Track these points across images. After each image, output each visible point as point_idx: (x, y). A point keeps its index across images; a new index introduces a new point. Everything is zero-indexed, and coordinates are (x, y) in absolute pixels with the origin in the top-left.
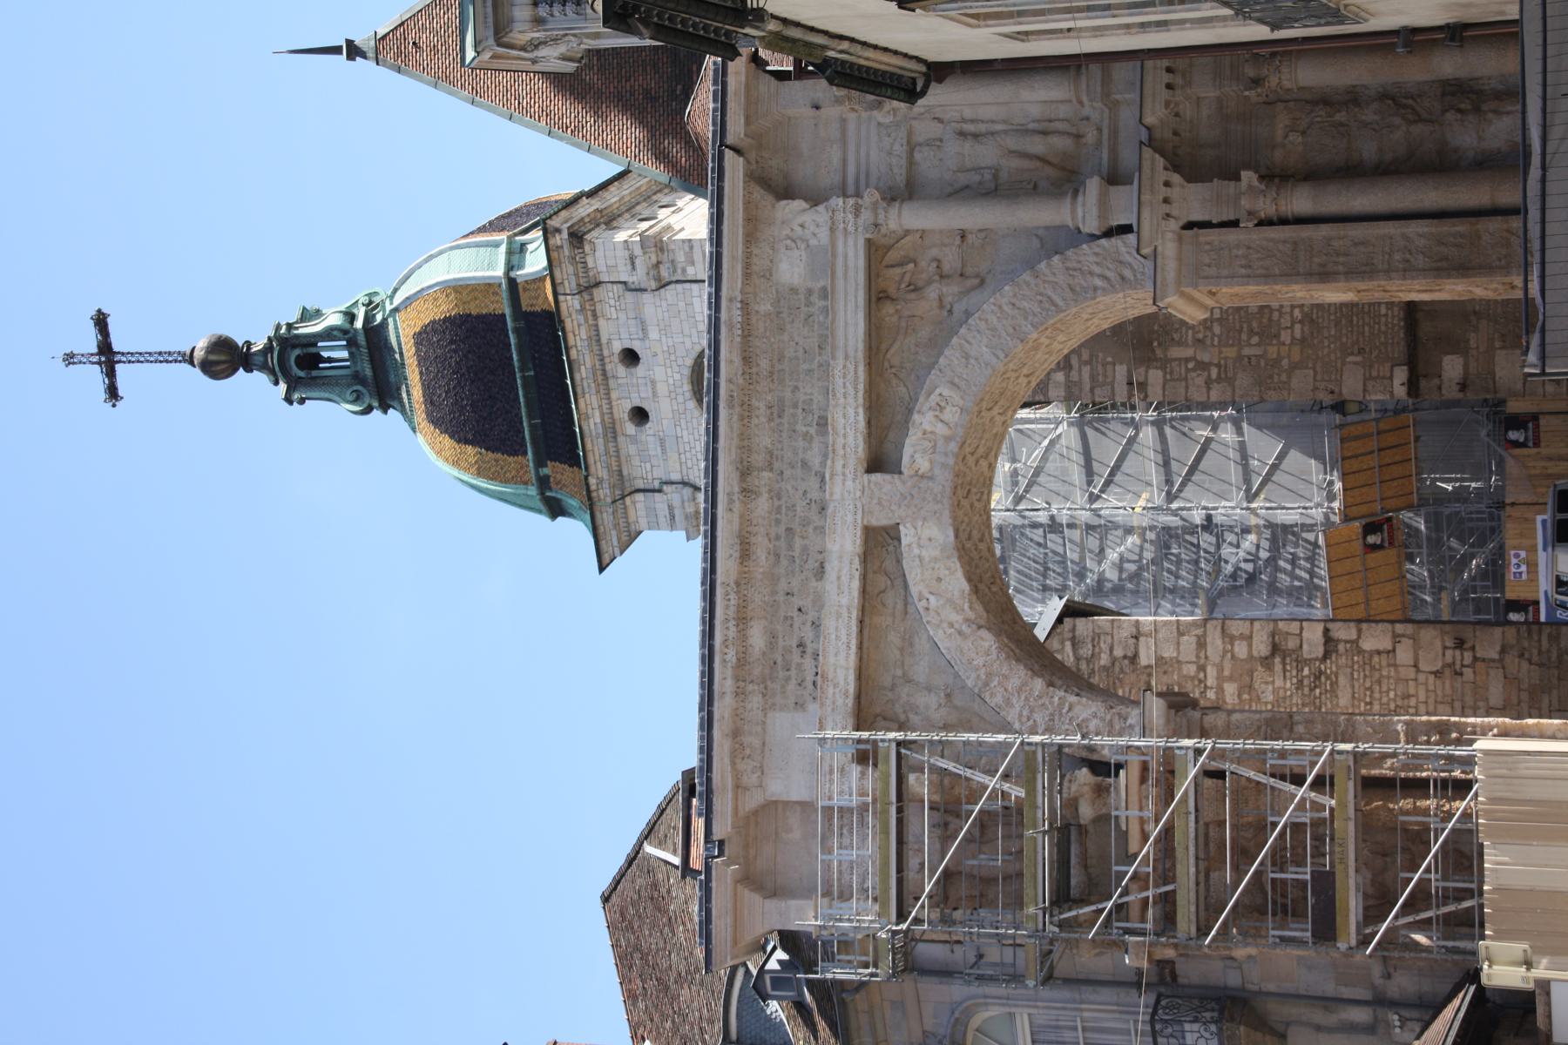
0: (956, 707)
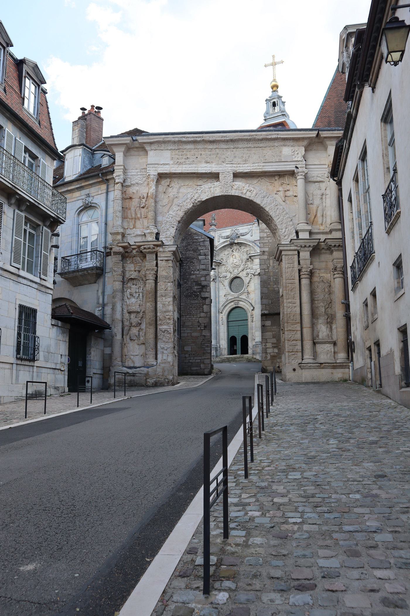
0: (173, 200)
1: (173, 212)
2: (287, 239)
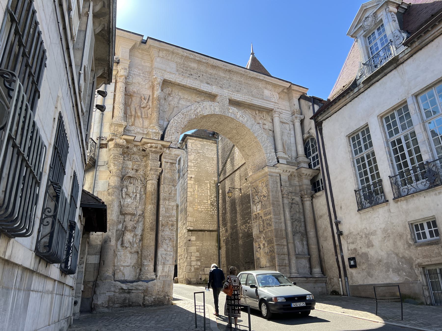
1: (178, 118)
2: (272, 162)
